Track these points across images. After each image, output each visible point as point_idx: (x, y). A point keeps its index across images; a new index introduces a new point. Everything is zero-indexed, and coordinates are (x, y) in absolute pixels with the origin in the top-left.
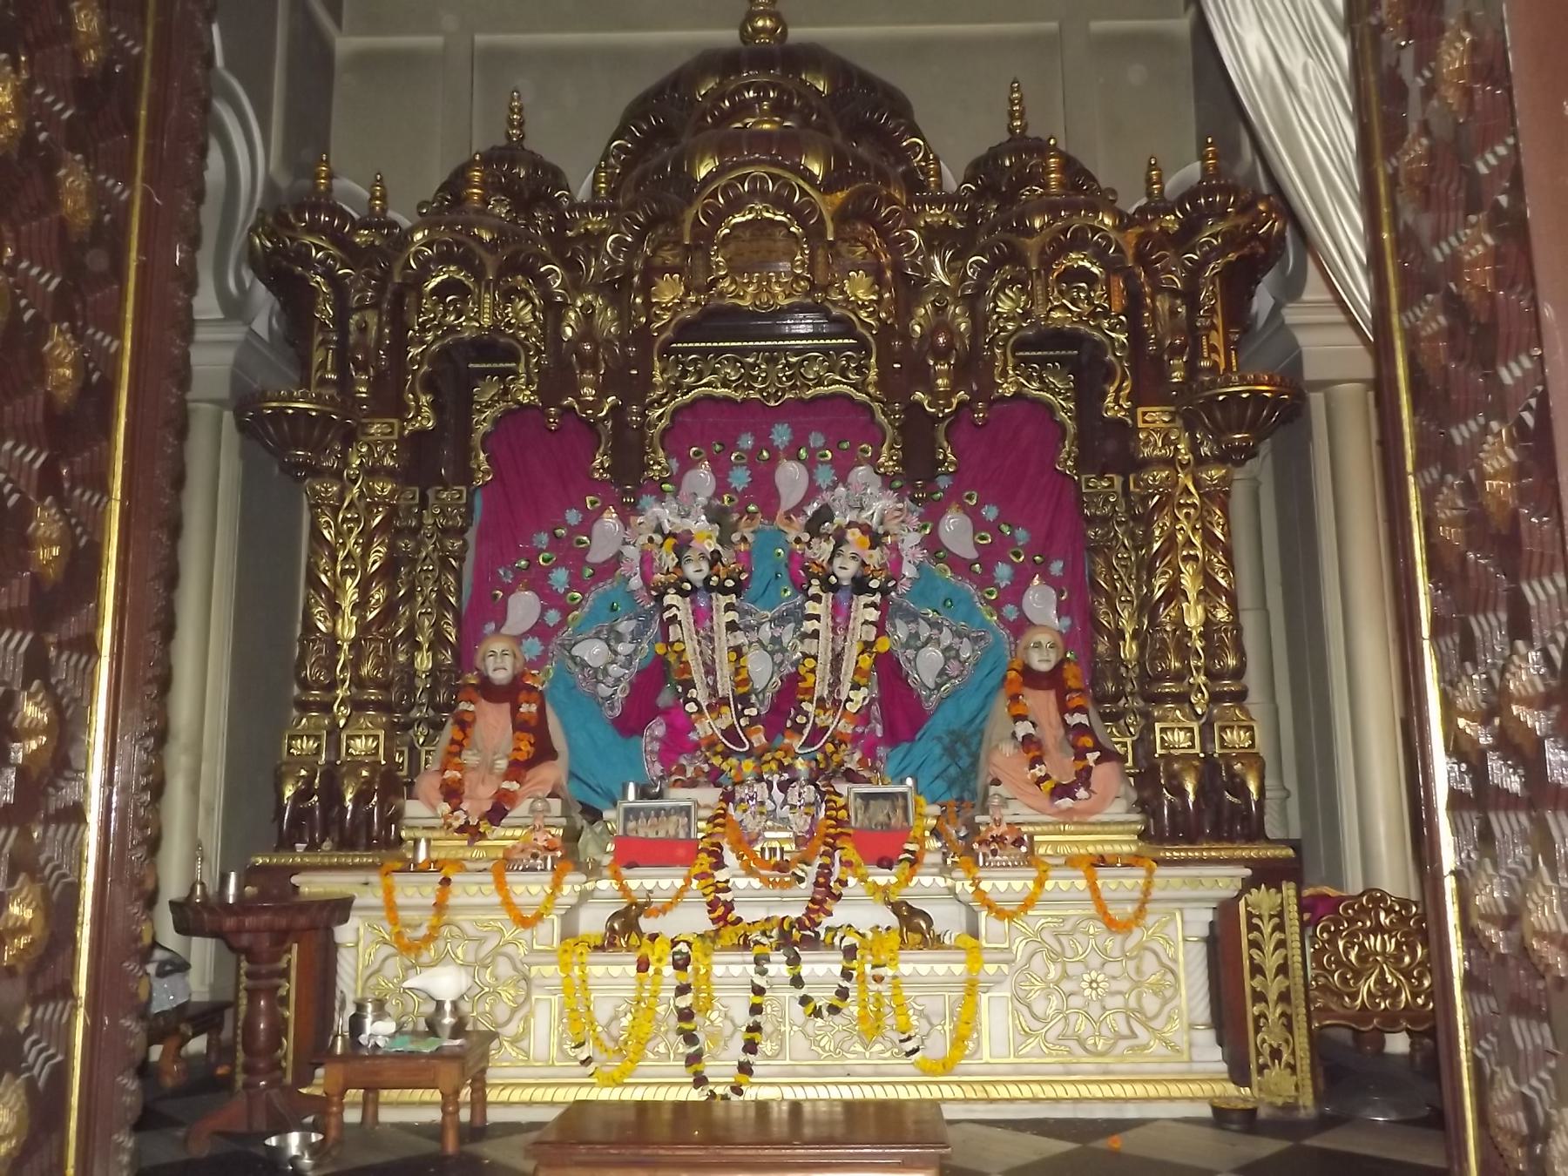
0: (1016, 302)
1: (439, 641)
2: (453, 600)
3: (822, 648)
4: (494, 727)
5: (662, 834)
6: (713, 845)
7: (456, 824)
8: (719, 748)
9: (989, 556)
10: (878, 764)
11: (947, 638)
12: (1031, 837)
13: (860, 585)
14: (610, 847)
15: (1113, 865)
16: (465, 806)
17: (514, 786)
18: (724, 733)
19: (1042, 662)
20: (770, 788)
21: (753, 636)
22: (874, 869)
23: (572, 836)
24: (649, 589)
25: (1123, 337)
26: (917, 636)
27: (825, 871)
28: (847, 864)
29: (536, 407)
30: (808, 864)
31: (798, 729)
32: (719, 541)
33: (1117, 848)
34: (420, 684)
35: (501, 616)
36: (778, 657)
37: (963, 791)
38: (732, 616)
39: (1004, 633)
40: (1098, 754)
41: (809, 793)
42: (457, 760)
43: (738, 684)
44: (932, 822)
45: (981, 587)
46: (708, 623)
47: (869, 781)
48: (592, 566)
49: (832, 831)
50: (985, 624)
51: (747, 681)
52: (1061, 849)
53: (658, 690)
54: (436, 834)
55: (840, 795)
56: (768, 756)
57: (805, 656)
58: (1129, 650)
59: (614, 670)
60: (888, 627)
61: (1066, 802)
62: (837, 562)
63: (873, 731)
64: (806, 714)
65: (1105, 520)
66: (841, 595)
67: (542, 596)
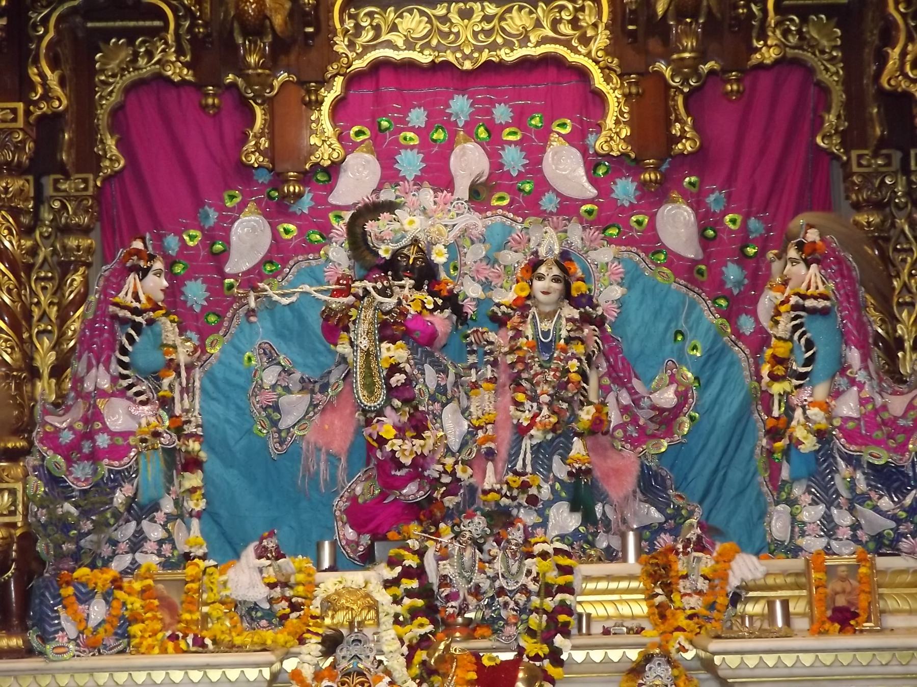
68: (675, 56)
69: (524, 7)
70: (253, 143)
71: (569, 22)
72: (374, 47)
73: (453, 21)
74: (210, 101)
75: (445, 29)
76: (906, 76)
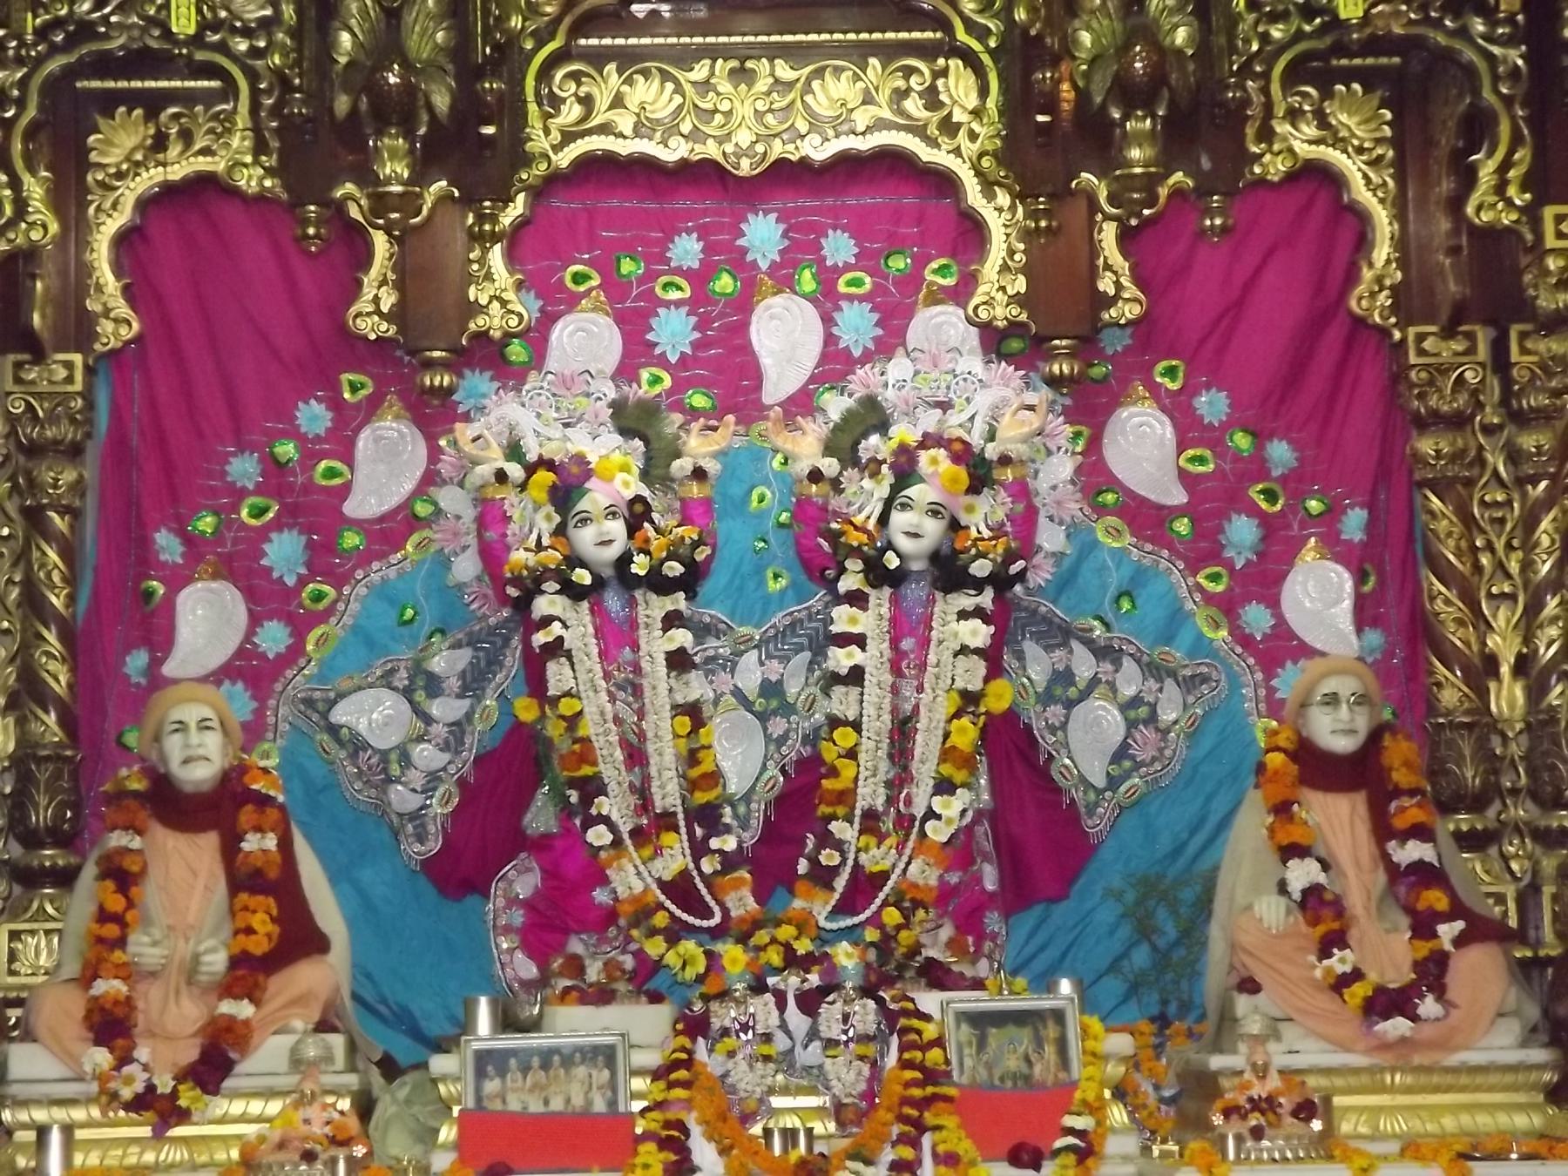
3: (873, 705)
4: (184, 880)
5: (557, 1105)
6: (668, 1125)
7: (127, 1093)
8: (660, 919)
9: (1213, 499)
11: (1130, 681)
12: (1327, 1100)
13: (948, 571)
14: (447, 1133)
15: (1499, 1156)
16: (142, 1053)
17: (244, 1009)
18: (663, 885)
19: (1336, 732)
20: (781, 1005)
21: (724, 681)
23: (365, 1107)
24: (499, 582)
26: (1064, 677)
30: (869, 1162)
31: (823, 877)
32: (645, 476)
33: (1503, 1119)
36: (778, 726)
37: (1165, 1002)
40: (1459, 925)
41: (866, 1015)
42: (118, 956)
43: (692, 785)
44: (1115, 1070)
47: (978, 984)
48: (358, 524)
49: (917, 1092)
50: (1200, 646)
51: (715, 778)
52: (1385, 1124)
53: (523, 801)
54: (78, 1114)
55: (927, 1018)
56: (762, 937)
57: (834, 722)
58: (1507, 697)
59: (427, 755)
61: (1398, 1026)
62: (898, 519)
63: (978, 880)
64: (839, 845)
65: (1458, 422)
66: (915, 591)
67: (250, 594)
68: (1118, 172)
69: (843, 69)
70: (371, 296)
71: (920, 94)
72: (583, 134)
73: (720, 89)
74: (311, 231)
76: (1509, 203)
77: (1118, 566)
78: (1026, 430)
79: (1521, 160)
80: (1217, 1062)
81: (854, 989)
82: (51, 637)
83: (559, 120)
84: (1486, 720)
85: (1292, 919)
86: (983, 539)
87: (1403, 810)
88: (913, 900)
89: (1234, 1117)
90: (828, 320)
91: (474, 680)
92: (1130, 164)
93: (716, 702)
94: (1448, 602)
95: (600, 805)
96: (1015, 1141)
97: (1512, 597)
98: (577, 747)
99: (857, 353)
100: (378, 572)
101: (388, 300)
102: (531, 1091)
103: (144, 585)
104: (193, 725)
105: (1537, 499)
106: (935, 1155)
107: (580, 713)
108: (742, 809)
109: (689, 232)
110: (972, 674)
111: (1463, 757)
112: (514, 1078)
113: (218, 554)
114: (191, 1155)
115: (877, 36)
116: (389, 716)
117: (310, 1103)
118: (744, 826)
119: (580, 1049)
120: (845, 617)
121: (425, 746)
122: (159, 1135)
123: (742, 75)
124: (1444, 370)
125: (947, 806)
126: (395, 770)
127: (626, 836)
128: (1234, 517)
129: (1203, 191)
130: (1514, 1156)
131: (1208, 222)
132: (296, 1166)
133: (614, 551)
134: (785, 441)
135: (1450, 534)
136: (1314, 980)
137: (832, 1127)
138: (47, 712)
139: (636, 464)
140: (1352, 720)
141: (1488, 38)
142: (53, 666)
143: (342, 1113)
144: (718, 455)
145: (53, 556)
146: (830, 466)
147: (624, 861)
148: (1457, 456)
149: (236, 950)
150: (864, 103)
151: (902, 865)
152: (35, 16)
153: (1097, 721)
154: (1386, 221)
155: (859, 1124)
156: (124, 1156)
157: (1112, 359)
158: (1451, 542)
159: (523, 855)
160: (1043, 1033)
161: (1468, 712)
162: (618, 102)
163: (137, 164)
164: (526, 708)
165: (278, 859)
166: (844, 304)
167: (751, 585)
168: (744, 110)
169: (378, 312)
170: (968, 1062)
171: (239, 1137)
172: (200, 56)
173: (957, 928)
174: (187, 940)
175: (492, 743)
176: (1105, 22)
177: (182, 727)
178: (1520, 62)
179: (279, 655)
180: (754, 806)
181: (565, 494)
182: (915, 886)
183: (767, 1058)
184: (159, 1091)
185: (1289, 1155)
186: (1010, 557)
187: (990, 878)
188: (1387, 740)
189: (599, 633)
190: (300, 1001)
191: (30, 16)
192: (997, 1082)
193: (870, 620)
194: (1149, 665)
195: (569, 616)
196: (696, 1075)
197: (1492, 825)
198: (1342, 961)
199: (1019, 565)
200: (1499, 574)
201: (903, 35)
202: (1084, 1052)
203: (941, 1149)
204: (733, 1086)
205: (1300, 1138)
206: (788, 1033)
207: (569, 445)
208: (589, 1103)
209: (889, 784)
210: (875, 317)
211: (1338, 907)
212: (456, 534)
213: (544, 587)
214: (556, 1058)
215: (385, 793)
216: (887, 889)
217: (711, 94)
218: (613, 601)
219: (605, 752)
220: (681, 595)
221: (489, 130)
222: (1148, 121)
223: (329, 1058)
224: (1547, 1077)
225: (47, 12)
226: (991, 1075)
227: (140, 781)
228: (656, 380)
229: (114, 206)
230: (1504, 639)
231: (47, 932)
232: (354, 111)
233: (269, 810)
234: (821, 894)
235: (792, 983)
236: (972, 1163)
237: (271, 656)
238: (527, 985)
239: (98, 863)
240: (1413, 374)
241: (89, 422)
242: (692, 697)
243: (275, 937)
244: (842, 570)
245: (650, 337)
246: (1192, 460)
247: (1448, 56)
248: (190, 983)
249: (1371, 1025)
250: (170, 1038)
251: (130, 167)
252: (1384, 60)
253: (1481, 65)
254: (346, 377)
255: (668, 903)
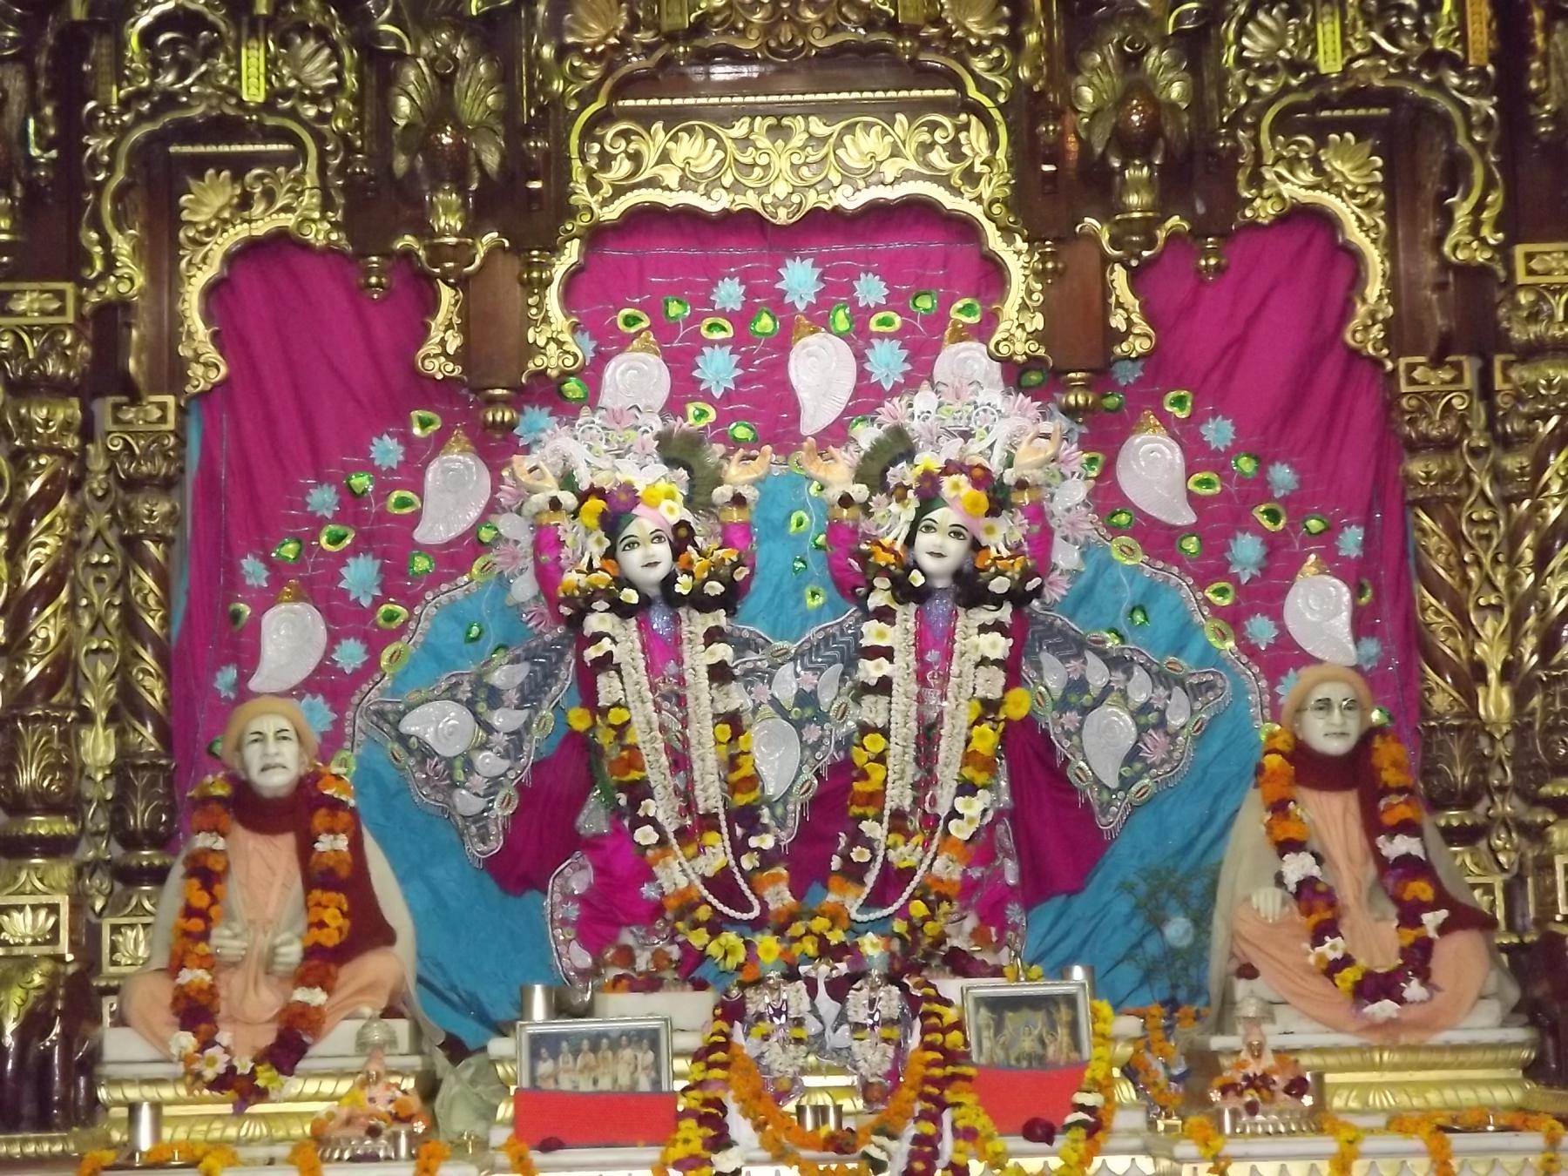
0: (1279, 38)
1: (127, 706)
2: (153, 623)
3: (900, 713)
5: (605, 1084)
7: (210, 1074)
8: (703, 913)
9: (1220, 518)
10: (1010, 934)
11: (1141, 689)
12: (1319, 1077)
13: (970, 588)
14: (505, 1110)
15: (1477, 1128)
16: (224, 1037)
17: (317, 997)
18: (707, 882)
19: (1329, 735)
21: (762, 691)
22: (1017, 1143)
23: (429, 1088)
25: (1488, 106)
26: (1079, 685)
27: (925, 1148)
28: (967, 1134)
29: (341, 253)
30: (892, 1137)
31: (855, 873)
32: (689, 502)
33: (1484, 1094)
34: (90, 791)
35: (246, 654)
36: (812, 732)
37: (1175, 987)
38: (722, 651)
39: (1251, 675)
40: (1443, 914)
41: (890, 1001)
42: (202, 948)
43: (734, 788)
44: (1124, 1051)
45: (1202, 582)
46: (671, 666)
47: (998, 972)
48: (427, 550)
49: (937, 1072)
50: (1209, 656)
51: (753, 781)
52: (1375, 1099)
54: (167, 1093)
55: (948, 1003)
56: (798, 928)
57: (865, 729)
58: (1495, 701)
59: (489, 762)
60: (1027, 671)
61: (1385, 1008)
62: (924, 540)
63: (1000, 873)
64: (869, 843)
65: (1447, 445)
67: (330, 615)
69: (873, 125)
70: (437, 340)
73: (759, 145)
75: (746, 159)
76: (1483, 241)
77: (1131, 583)
78: (1042, 456)
79: (1495, 201)
80: (1217, 1042)
81: (879, 976)
82: (147, 656)
83: (611, 175)
84: (1475, 722)
85: (1287, 909)
86: (1001, 558)
87: (1391, 807)
88: (937, 893)
89: (1231, 1093)
90: (860, 357)
91: (532, 692)
92: (1128, 209)
93: (755, 711)
94: (1438, 613)
95: (647, 807)
96: (1032, 1115)
97: (1498, 609)
98: (625, 753)
99: (888, 387)
100: (446, 594)
101: (454, 343)
102: (581, 1071)
103: (232, 607)
104: (271, 735)
105: (1520, 517)
106: (954, 1130)
107: (629, 722)
108: (779, 811)
109: (731, 277)
110: (992, 683)
111: (1453, 757)
112: (566, 1059)
113: (300, 578)
114: (269, 1130)
115: (904, 94)
116: (453, 726)
117: (376, 1083)
118: (782, 824)
119: (624, 1033)
120: (874, 632)
121: (488, 753)
122: (239, 1112)
123: (779, 131)
124: (1431, 398)
125: (969, 806)
126: (459, 775)
127: (671, 836)
128: (1239, 535)
129: (1199, 233)
130: (1491, 1128)
131: (1203, 263)
132: (362, 1140)
133: (660, 572)
134: (817, 468)
135: (1439, 550)
136: (1309, 965)
137: (860, 1104)
138: (145, 725)
139: (681, 492)
140: (1344, 724)
141: (1459, 89)
142: (149, 682)
143: (405, 1092)
144: (754, 483)
145: (149, 581)
146: (860, 492)
147: (670, 859)
148: (1446, 478)
149: (310, 943)
150: (892, 156)
151: (927, 861)
152: (119, 89)
153: (1110, 725)
154: (1378, 259)
155: (884, 1101)
156: (208, 1131)
157: (1125, 390)
158: (1441, 558)
159: (578, 854)
160: (1056, 1016)
161: (1457, 716)
162: (664, 158)
163: (225, 221)
164: (579, 718)
165: (349, 858)
166: (875, 342)
167: (792, 603)
168: (781, 164)
169: (445, 354)
170: (986, 1044)
171: (312, 1114)
172: (271, 121)
173: (982, 919)
174: (265, 933)
175: (547, 752)
176: (1106, 79)
177: (261, 737)
178: (1492, 112)
179: (355, 670)
180: (790, 807)
181: (613, 523)
182: (941, 881)
183: (799, 1041)
184: (239, 1072)
185: (1282, 1129)
186: (1027, 575)
187: (1011, 873)
188: (1377, 742)
189: (645, 649)
190: (369, 988)
191: (114, 89)
192: (1013, 1062)
193: (897, 634)
194: (1158, 674)
195: (618, 631)
196: (734, 1056)
197: (1481, 820)
198: (1333, 947)
199: (1036, 582)
200: (1486, 587)
201: (928, 93)
202: (1095, 1034)
203: (960, 1124)
204: (767, 1066)
205: (1292, 1112)
206: (819, 1018)
207: (618, 475)
208: (635, 1082)
209: (914, 786)
210: (905, 353)
211: (1330, 898)
212: (515, 558)
213: (594, 606)
214: (605, 1041)
215: (451, 797)
216: (913, 884)
217: (751, 149)
218: (659, 622)
219: (651, 758)
220: (722, 612)
221: (536, 185)
222: (1145, 170)
223: (392, 1042)
224: (1525, 1054)
225: (130, 85)
226: (1007, 1057)
227: (223, 787)
228: (703, 414)
229: (204, 259)
230: (1491, 647)
231: (145, 926)
232: (411, 171)
233: (340, 814)
234: (852, 889)
235: (823, 971)
236: (989, 1138)
237: (348, 671)
238: (584, 974)
239: (185, 864)
240: (1404, 402)
241: (181, 457)
242: (732, 708)
243: (345, 930)
244: (872, 588)
245: (696, 373)
246: (1200, 483)
247: (1423, 107)
248: (268, 973)
249: (1360, 1007)
250: (249, 1023)
251: (218, 225)
252: (1374, 111)
253: (1457, 115)
254: (416, 414)
255: (711, 898)
